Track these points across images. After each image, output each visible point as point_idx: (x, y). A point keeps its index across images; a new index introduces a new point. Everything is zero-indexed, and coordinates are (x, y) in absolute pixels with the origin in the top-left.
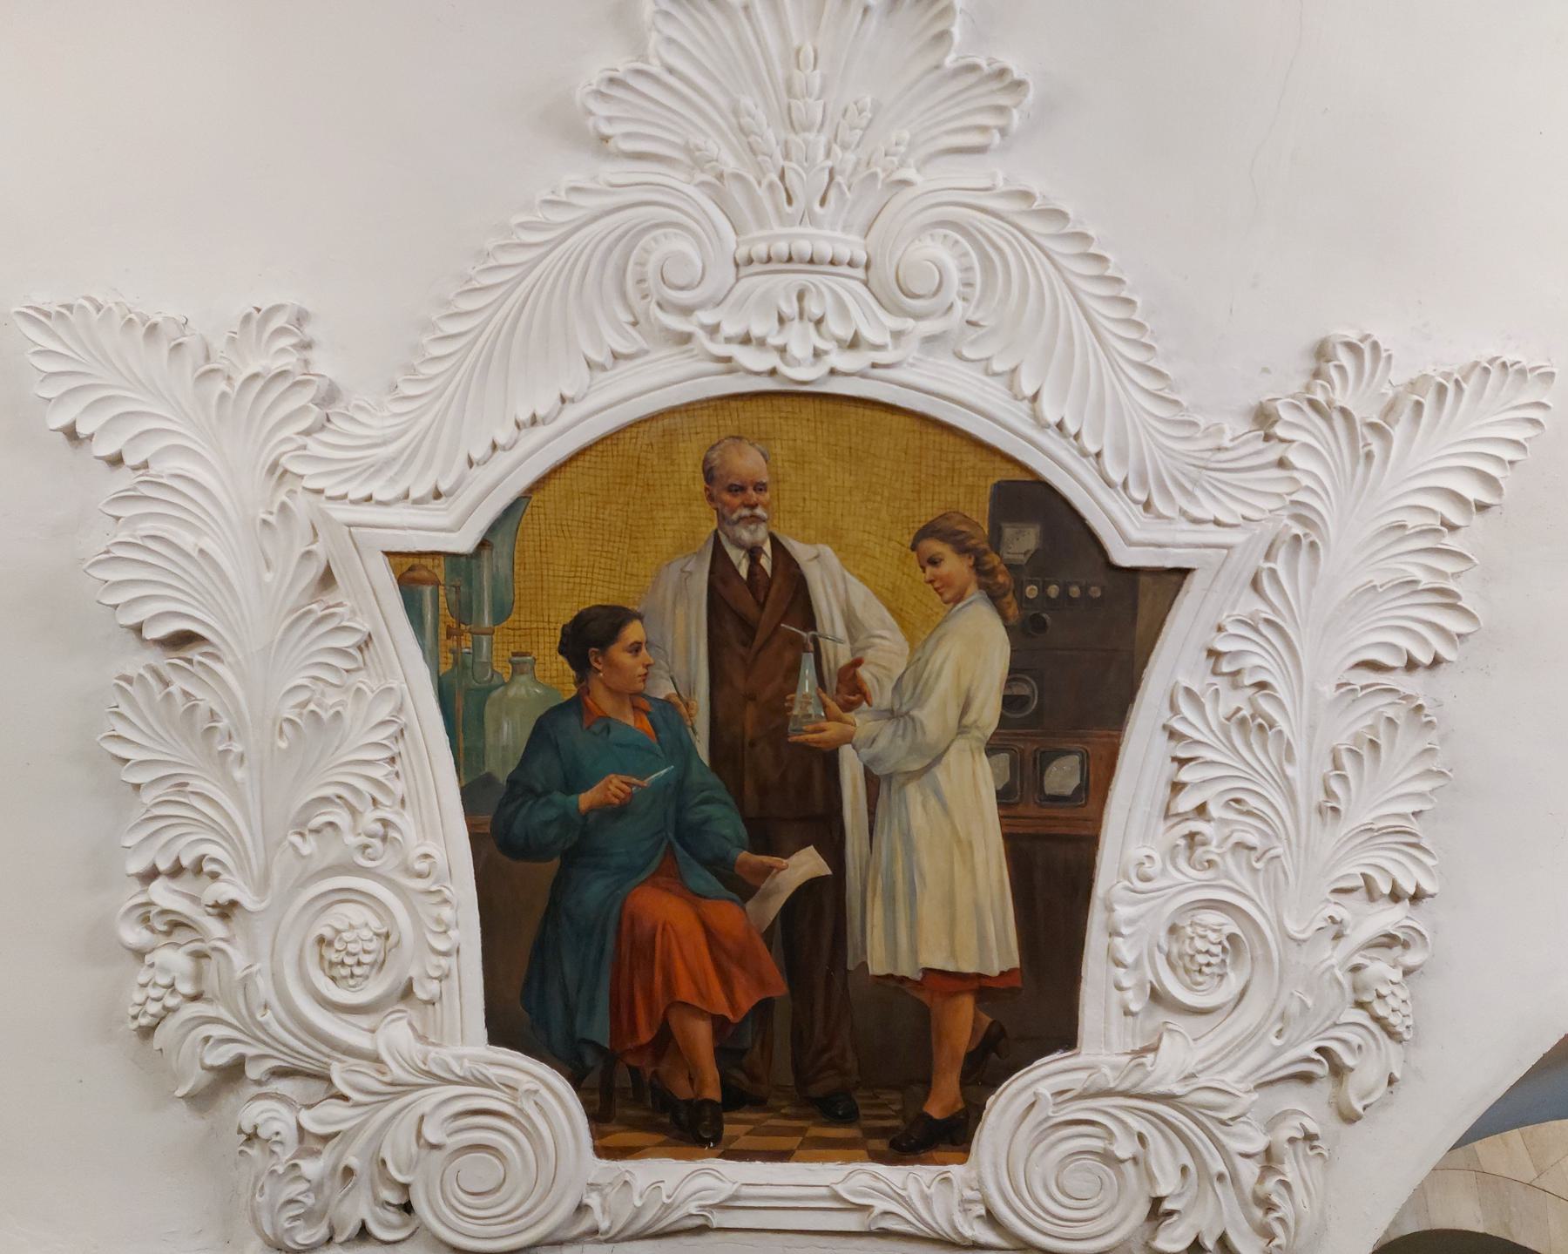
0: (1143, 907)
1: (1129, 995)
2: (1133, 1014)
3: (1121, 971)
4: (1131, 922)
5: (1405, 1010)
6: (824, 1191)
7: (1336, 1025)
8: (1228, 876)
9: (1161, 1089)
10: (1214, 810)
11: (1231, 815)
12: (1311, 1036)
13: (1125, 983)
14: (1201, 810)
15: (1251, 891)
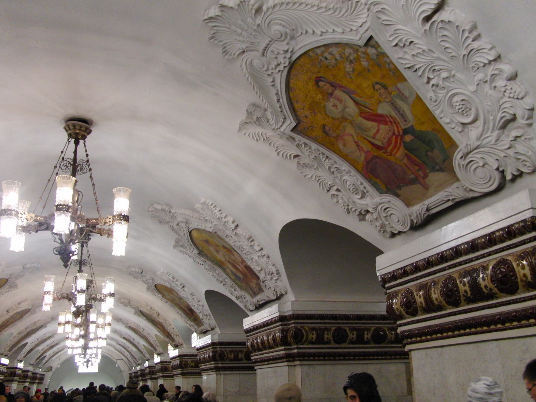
0: (441, 107)
1: (456, 128)
2: (463, 131)
3: (449, 125)
4: (442, 112)
5: (513, 91)
6: (440, 200)
7: (501, 106)
8: (450, 87)
9: (475, 146)
10: (431, 76)
11: (436, 74)
12: (498, 112)
13: (453, 126)
14: (429, 79)
15: (457, 86)
